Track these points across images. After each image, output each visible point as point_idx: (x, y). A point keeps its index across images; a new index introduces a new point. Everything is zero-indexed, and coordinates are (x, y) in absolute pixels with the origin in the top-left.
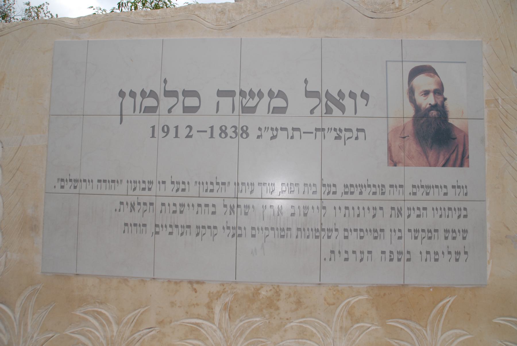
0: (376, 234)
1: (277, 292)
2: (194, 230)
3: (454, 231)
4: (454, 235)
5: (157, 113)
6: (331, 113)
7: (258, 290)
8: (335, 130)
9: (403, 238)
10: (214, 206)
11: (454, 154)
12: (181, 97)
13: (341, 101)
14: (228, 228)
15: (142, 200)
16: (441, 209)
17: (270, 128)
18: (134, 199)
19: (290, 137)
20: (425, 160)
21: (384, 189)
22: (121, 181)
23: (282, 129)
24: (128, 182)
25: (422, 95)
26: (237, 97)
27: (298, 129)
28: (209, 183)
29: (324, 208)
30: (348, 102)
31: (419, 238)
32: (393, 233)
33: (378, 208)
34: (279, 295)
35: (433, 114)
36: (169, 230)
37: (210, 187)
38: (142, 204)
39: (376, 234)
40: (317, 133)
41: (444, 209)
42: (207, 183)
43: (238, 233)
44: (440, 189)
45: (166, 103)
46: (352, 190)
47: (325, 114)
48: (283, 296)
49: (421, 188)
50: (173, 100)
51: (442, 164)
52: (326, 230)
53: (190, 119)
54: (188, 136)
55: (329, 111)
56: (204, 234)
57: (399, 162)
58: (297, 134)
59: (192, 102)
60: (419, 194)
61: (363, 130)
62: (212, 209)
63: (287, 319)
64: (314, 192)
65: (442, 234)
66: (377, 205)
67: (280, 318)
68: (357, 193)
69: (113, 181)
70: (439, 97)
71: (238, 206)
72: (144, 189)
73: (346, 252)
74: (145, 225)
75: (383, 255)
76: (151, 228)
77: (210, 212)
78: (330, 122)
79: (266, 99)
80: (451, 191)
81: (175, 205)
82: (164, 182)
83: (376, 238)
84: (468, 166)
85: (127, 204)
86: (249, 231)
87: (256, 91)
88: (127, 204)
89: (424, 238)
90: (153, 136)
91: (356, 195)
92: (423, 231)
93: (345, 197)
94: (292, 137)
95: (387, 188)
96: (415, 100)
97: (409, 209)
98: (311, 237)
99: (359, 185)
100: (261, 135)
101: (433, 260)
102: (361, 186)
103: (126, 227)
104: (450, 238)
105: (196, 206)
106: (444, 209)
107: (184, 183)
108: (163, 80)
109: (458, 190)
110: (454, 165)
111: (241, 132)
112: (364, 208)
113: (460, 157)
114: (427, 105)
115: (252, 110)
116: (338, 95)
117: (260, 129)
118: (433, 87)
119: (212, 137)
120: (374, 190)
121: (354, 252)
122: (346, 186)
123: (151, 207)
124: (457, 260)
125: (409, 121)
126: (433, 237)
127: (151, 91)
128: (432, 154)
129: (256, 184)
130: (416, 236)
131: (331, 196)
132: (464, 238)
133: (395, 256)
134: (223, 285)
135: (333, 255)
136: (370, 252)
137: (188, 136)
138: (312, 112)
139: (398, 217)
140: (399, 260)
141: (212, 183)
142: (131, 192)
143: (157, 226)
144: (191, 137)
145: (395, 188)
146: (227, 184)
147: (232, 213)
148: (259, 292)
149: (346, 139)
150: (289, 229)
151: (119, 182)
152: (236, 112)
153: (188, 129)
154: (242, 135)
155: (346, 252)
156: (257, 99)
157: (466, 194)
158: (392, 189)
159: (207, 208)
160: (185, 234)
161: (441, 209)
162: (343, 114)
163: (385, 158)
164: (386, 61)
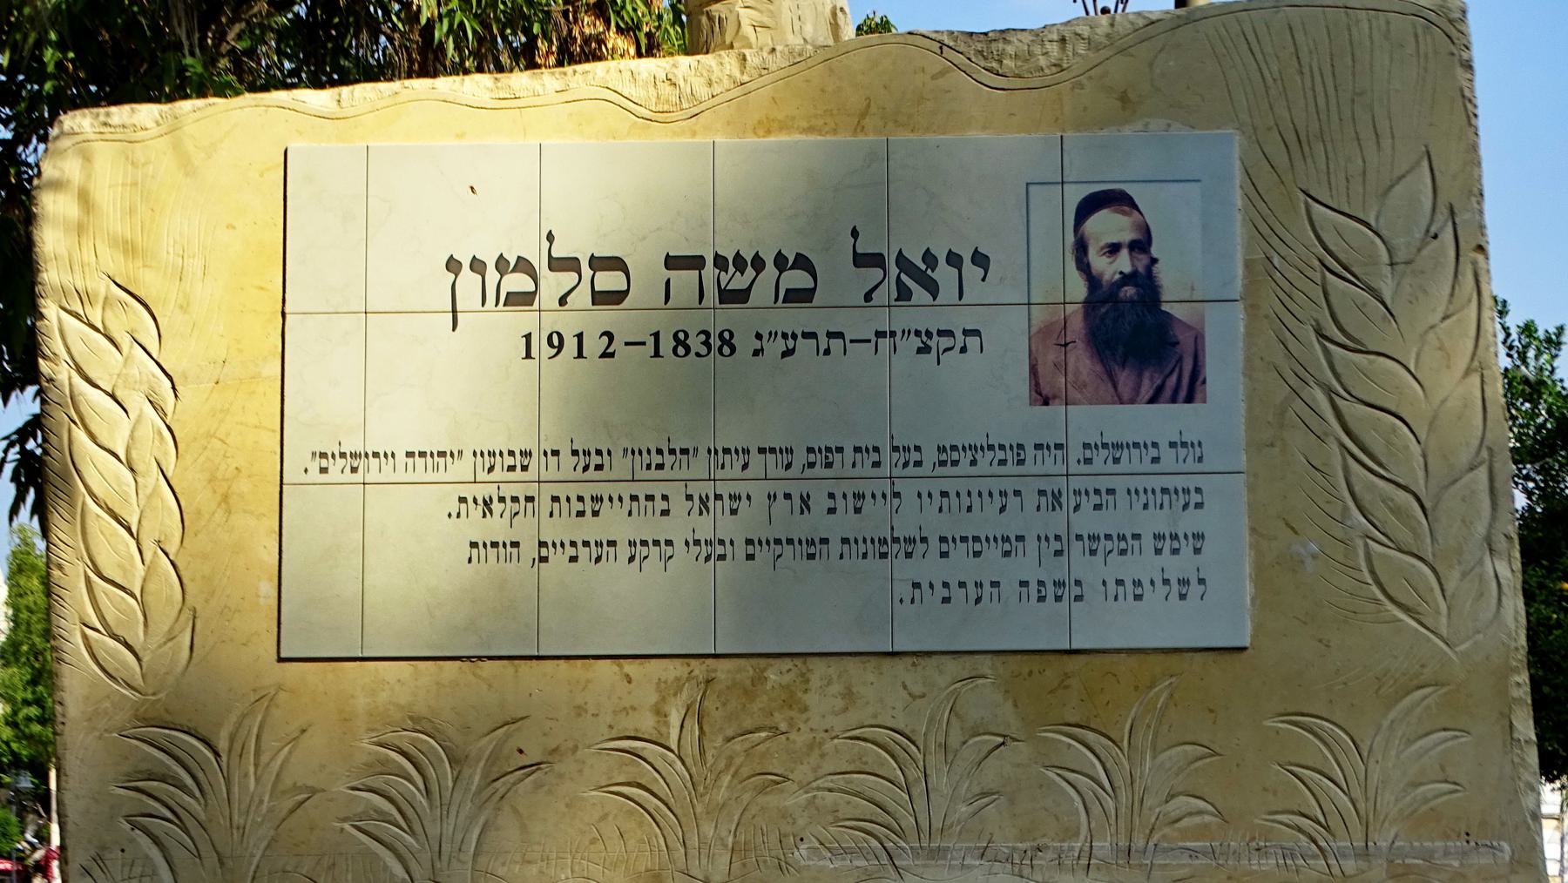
0: (1007, 547)
1: (803, 675)
2: (624, 551)
8: (918, 333)
9: (1066, 553)
10: (665, 498)
11: (1174, 378)
12: (586, 271)
13: (929, 272)
14: (697, 543)
15: (508, 491)
16: (1145, 491)
17: (780, 334)
18: (491, 490)
19: (821, 351)
20: (1112, 390)
22: (460, 453)
23: (806, 335)
24: (475, 454)
25: (1104, 254)
26: (710, 270)
27: (840, 335)
28: (653, 452)
29: (897, 495)
30: (944, 275)
31: (1100, 552)
33: (1011, 493)
34: (808, 681)
35: (1128, 295)
36: (571, 551)
37: (657, 459)
38: (508, 500)
39: (1007, 547)
41: (1153, 491)
42: (649, 452)
43: (718, 552)
46: (955, 456)
47: (896, 300)
51: (1147, 397)
54: (604, 355)
55: (904, 294)
57: (1055, 397)
58: (836, 344)
61: (976, 333)
62: (662, 505)
63: (826, 731)
64: (876, 464)
65: (1148, 542)
66: (1009, 485)
67: (812, 730)
69: (442, 454)
70: (1142, 256)
71: (718, 497)
72: (512, 468)
73: (946, 585)
74: (515, 544)
75: (1025, 589)
76: (529, 550)
77: (658, 512)
78: (904, 318)
80: (1168, 455)
81: (580, 499)
82: (555, 453)
83: (1007, 554)
84: (1205, 402)
85: (475, 501)
88: (475, 501)
89: (1110, 552)
90: (528, 356)
91: (964, 468)
92: (1108, 537)
93: (940, 471)
94: (827, 352)
95: (1030, 451)
96: (1088, 265)
97: (1077, 493)
99: (970, 446)
100: (762, 349)
101: (1130, 597)
103: (475, 551)
104: (1166, 550)
105: (626, 499)
107: (599, 452)
109: (1182, 452)
110: (1174, 400)
111: (719, 343)
112: (980, 494)
114: (1115, 273)
115: (742, 296)
117: (759, 336)
118: (1127, 236)
119: (657, 354)
120: (1000, 455)
121: (962, 585)
122: (942, 449)
123: (530, 505)
124: (1183, 597)
125: (1075, 311)
128: (1125, 378)
129: (754, 451)
131: (911, 470)
132: (1197, 551)
133: (1050, 591)
136: (995, 584)
138: (868, 297)
139: (1054, 509)
140: (1058, 598)
141: (660, 452)
143: (542, 544)
144: (612, 355)
145: (1045, 450)
148: (765, 674)
149: (941, 352)
150: (825, 541)
152: (706, 302)
153: (605, 339)
154: (720, 350)
156: (750, 272)
157: (1200, 459)
160: (604, 557)
162: (934, 299)
163: (1023, 388)
164: (1028, 184)
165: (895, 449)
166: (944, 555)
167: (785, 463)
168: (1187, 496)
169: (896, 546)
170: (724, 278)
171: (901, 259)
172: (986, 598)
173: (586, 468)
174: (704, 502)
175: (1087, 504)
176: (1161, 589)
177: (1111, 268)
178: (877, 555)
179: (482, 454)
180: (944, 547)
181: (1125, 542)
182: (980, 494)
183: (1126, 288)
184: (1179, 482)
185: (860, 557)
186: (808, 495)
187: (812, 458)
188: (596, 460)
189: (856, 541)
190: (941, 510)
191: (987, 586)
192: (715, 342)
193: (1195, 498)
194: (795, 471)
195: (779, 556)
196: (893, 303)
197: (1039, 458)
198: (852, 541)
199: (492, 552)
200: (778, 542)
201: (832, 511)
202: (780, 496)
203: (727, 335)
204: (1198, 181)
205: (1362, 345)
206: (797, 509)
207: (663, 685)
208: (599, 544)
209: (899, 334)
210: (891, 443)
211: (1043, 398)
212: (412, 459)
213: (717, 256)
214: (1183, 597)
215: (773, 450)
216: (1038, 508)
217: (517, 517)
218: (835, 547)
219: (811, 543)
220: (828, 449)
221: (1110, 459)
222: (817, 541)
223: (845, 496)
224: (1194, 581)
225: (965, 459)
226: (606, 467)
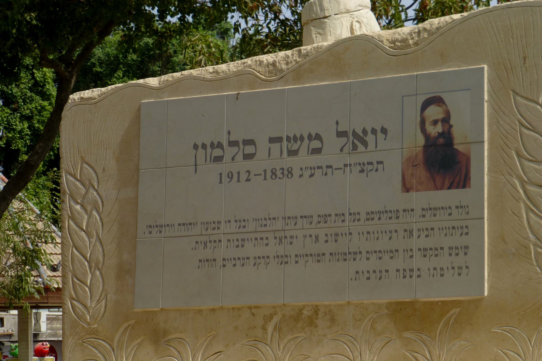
0: (392, 255)
2: (252, 261)
3: (457, 248)
4: (457, 251)
6: (357, 150)
7: (301, 310)
8: (360, 164)
14: (278, 257)
15: (213, 238)
16: (446, 228)
18: (207, 238)
19: (324, 174)
21: (398, 213)
22: (197, 223)
26: (285, 143)
29: (350, 234)
30: (370, 138)
32: (406, 252)
34: (317, 314)
37: (264, 222)
38: (212, 242)
39: (392, 255)
40: (346, 168)
41: (449, 228)
42: (262, 219)
44: (445, 210)
45: (230, 152)
46: (373, 216)
47: (352, 150)
48: (321, 314)
49: (429, 210)
50: (235, 149)
51: (448, 186)
52: (352, 253)
54: (248, 180)
55: (355, 147)
56: (260, 264)
57: (411, 188)
58: (329, 170)
59: (249, 149)
60: (428, 216)
62: (265, 241)
63: (324, 336)
65: (446, 250)
67: (319, 335)
68: (376, 218)
69: (190, 224)
71: (286, 237)
72: (214, 229)
73: (368, 272)
74: (214, 260)
75: (398, 273)
76: (220, 262)
79: (306, 141)
80: (454, 211)
81: (237, 240)
83: (392, 258)
84: (470, 187)
85: (201, 242)
86: (293, 259)
89: (432, 255)
90: (221, 182)
91: (376, 221)
92: (431, 249)
93: (367, 222)
94: (326, 174)
95: (401, 212)
97: (419, 230)
98: (340, 260)
99: (378, 211)
101: (439, 275)
102: (380, 212)
104: (453, 254)
105: (253, 240)
106: (449, 228)
107: (244, 220)
109: (460, 210)
110: (457, 187)
111: (287, 173)
112: (382, 232)
113: (462, 179)
114: (435, 133)
115: (292, 153)
116: (363, 132)
117: (301, 169)
118: (441, 116)
119: (265, 179)
120: (390, 215)
121: (374, 272)
122: (368, 213)
126: (439, 255)
127: (218, 142)
129: (299, 217)
130: (425, 254)
131: (356, 223)
132: (466, 254)
133: (408, 273)
134: (275, 308)
135: (357, 275)
136: (387, 271)
137: (248, 180)
138: (342, 150)
139: (410, 238)
141: (265, 219)
143: (224, 259)
145: (407, 212)
146: (277, 219)
147: (281, 244)
148: (302, 312)
150: (324, 254)
153: (247, 174)
156: (299, 142)
157: (468, 213)
158: (405, 213)
159: (262, 241)
160: (245, 264)
161: (446, 228)
162: (366, 149)
163: (399, 186)
165: (350, 214)
166: (368, 259)
167: (310, 222)
169: (350, 256)
170: (290, 145)
172: (383, 277)
173: (240, 227)
174: (280, 240)
175: (423, 235)
176: (451, 271)
177: (434, 130)
178: (343, 260)
181: (437, 251)
182: (382, 232)
183: (440, 139)
185: (337, 261)
186: (318, 235)
191: (384, 271)
192: (286, 172)
193: (465, 230)
194: (313, 225)
196: (351, 152)
198: (334, 254)
199: (206, 263)
200: (307, 255)
201: (326, 241)
202: (308, 236)
203: (290, 169)
204: (469, 89)
205: (535, 158)
206: (314, 241)
208: (243, 259)
209: (353, 165)
210: (349, 212)
211: (406, 189)
212: (191, 226)
213: (287, 136)
214: (459, 274)
215: (305, 217)
216: (404, 238)
218: (328, 257)
219: (319, 255)
220: (326, 215)
221: (432, 215)
222: (321, 254)
223: (331, 235)
224: (464, 268)
225: (376, 217)
226: (247, 226)
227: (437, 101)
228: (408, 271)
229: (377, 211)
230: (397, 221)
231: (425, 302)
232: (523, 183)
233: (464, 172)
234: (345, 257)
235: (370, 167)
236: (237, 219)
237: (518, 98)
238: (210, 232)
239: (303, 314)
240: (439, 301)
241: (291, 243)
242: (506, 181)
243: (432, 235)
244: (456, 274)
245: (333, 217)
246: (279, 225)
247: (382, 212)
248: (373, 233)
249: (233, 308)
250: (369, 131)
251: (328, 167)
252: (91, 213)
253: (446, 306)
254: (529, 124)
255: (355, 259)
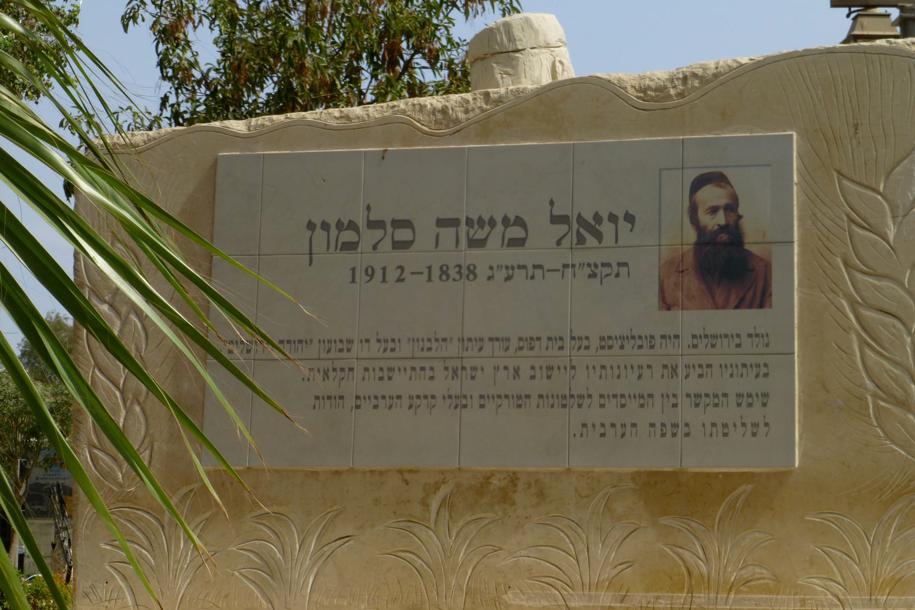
0: (642, 401)
1: (512, 481)
2: (406, 402)
3: (750, 395)
4: (750, 400)
5: (359, 250)
7: (488, 478)
8: (589, 265)
11: (751, 292)
12: (389, 229)
13: (597, 226)
14: (450, 397)
15: (338, 365)
16: (731, 366)
17: (504, 266)
18: (329, 364)
22: (311, 340)
23: (520, 267)
24: (320, 341)
25: (708, 213)
26: (463, 227)
27: (540, 267)
29: (573, 368)
30: (607, 228)
32: (666, 399)
34: (516, 485)
35: (723, 239)
36: (374, 402)
37: (427, 345)
38: (338, 370)
39: (642, 401)
40: (566, 270)
41: (737, 366)
42: (423, 340)
44: (731, 340)
45: (369, 237)
46: (610, 343)
47: (576, 244)
48: (521, 486)
50: (379, 233)
53: (400, 257)
54: (400, 280)
55: (581, 240)
57: (674, 305)
58: (538, 272)
59: (403, 235)
63: (527, 518)
64: (561, 348)
65: (732, 398)
66: (644, 361)
67: (517, 517)
69: (300, 342)
71: (463, 368)
72: (341, 350)
73: (603, 425)
74: (341, 397)
75: (652, 429)
76: (351, 402)
77: (427, 377)
78: (579, 257)
79: (500, 227)
80: (746, 341)
81: (381, 369)
82: (367, 341)
83: (642, 406)
84: (771, 307)
85: (319, 370)
86: (476, 401)
87: (486, 219)
88: (319, 370)
89: (708, 405)
90: (353, 281)
91: (616, 349)
92: (707, 395)
93: (600, 352)
94: (533, 277)
95: (658, 340)
96: (698, 221)
97: (688, 366)
98: (556, 405)
99: (620, 336)
101: (720, 435)
102: (622, 338)
103: (317, 402)
105: (409, 370)
107: (393, 340)
108: (366, 206)
109: (756, 340)
110: (751, 306)
111: (467, 272)
112: (626, 367)
113: (759, 294)
114: (714, 226)
115: (479, 244)
117: (491, 268)
118: (723, 201)
119: (430, 279)
120: (639, 342)
121: (613, 425)
122: (602, 339)
123: (351, 373)
124: (754, 434)
125: (688, 248)
127: (350, 221)
129: (486, 339)
130: (697, 402)
131: (583, 352)
132: (764, 405)
133: (669, 430)
134: (443, 474)
135: (585, 429)
136: (634, 425)
137: (400, 280)
138: (559, 243)
139: (672, 377)
140: (674, 435)
141: (429, 340)
142: (324, 355)
143: (357, 397)
144: (403, 280)
146: (448, 340)
148: (490, 481)
150: (528, 396)
151: (309, 342)
153: (399, 270)
154: (468, 277)
155: (603, 425)
156: (487, 228)
157: (767, 345)
158: (664, 341)
159: (423, 372)
160: (394, 406)
161: (731, 366)
162: (600, 243)
163: (655, 299)
164: (660, 170)
165: (573, 338)
166: (602, 406)
167: (505, 347)
168: (758, 369)
169: (572, 400)
170: (472, 232)
171: (580, 219)
173: (385, 350)
175: (694, 374)
176: (741, 430)
178: (560, 406)
179: (324, 342)
180: (602, 401)
181: (717, 399)
182: (626, 367)
183: (722, 235)
184: (753, 360)
185: (550, 406)
186: (518, 368)
187: (521, 344)
188: (391, 345)
189: (547, 397)
190: (601, 377)
192: (465, 272)
193: (763, 370)
194: (511, 352)
195: (500, 406)
197: (664, 345)
198: (545, 397)
199: (327, 402)
200: (499, 397)
201: (533, 377)
203: (472, 268)
204: (769, 165)
207: (427, 486)
208: (391, 397)
209: (577, 266)
210: (571, 335)
211: (666, 305)
213: (467, 218)
214: (754, 434)
215: (497, 339)
216: (662, 376)
217: (343, 381)
218: (534, 400)
219: (519, 397)
220: (532, 339)
221: (709, 345)
222: (523, 396)
223: (541, 368)
225: (617, 345)
226: (397, 350)
227: (717, 178)
228: (669, 428)
229: (618, 336)
230: (651, 351)
231: (696, 474)
232: (853, 304)
233: (761, 284)
234: (564, 402)
235: (606, 271)
236: (380, 337)
237: (846, 183)
238: (332, 355)
239: (490, 483)
240: (720, 473)
241: (473, 378)
242: (829, 301)
243: (709, 374)
244: (749, 433)
245: (544, 342)
246: (453, 349)
247: (625, 337)
248: (612, 367)
249: (372, 472)
250: (605, 216)
251: (535, 267)
252: (127, 318)
253: (730, 480)
254: (864, 221)
255: (580, 406)
